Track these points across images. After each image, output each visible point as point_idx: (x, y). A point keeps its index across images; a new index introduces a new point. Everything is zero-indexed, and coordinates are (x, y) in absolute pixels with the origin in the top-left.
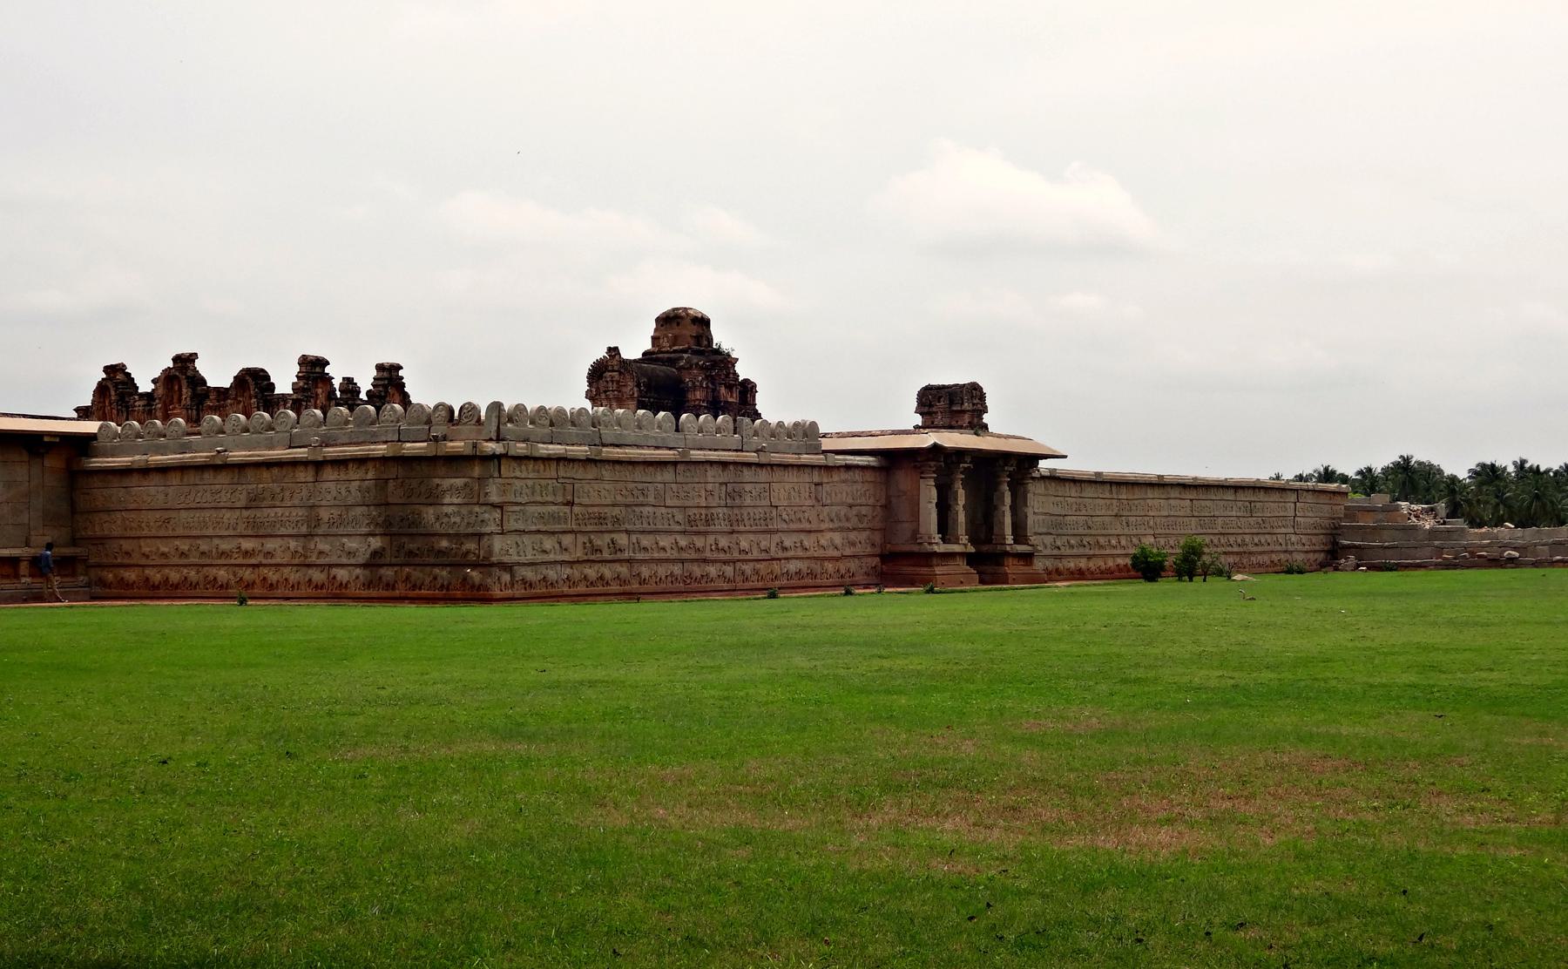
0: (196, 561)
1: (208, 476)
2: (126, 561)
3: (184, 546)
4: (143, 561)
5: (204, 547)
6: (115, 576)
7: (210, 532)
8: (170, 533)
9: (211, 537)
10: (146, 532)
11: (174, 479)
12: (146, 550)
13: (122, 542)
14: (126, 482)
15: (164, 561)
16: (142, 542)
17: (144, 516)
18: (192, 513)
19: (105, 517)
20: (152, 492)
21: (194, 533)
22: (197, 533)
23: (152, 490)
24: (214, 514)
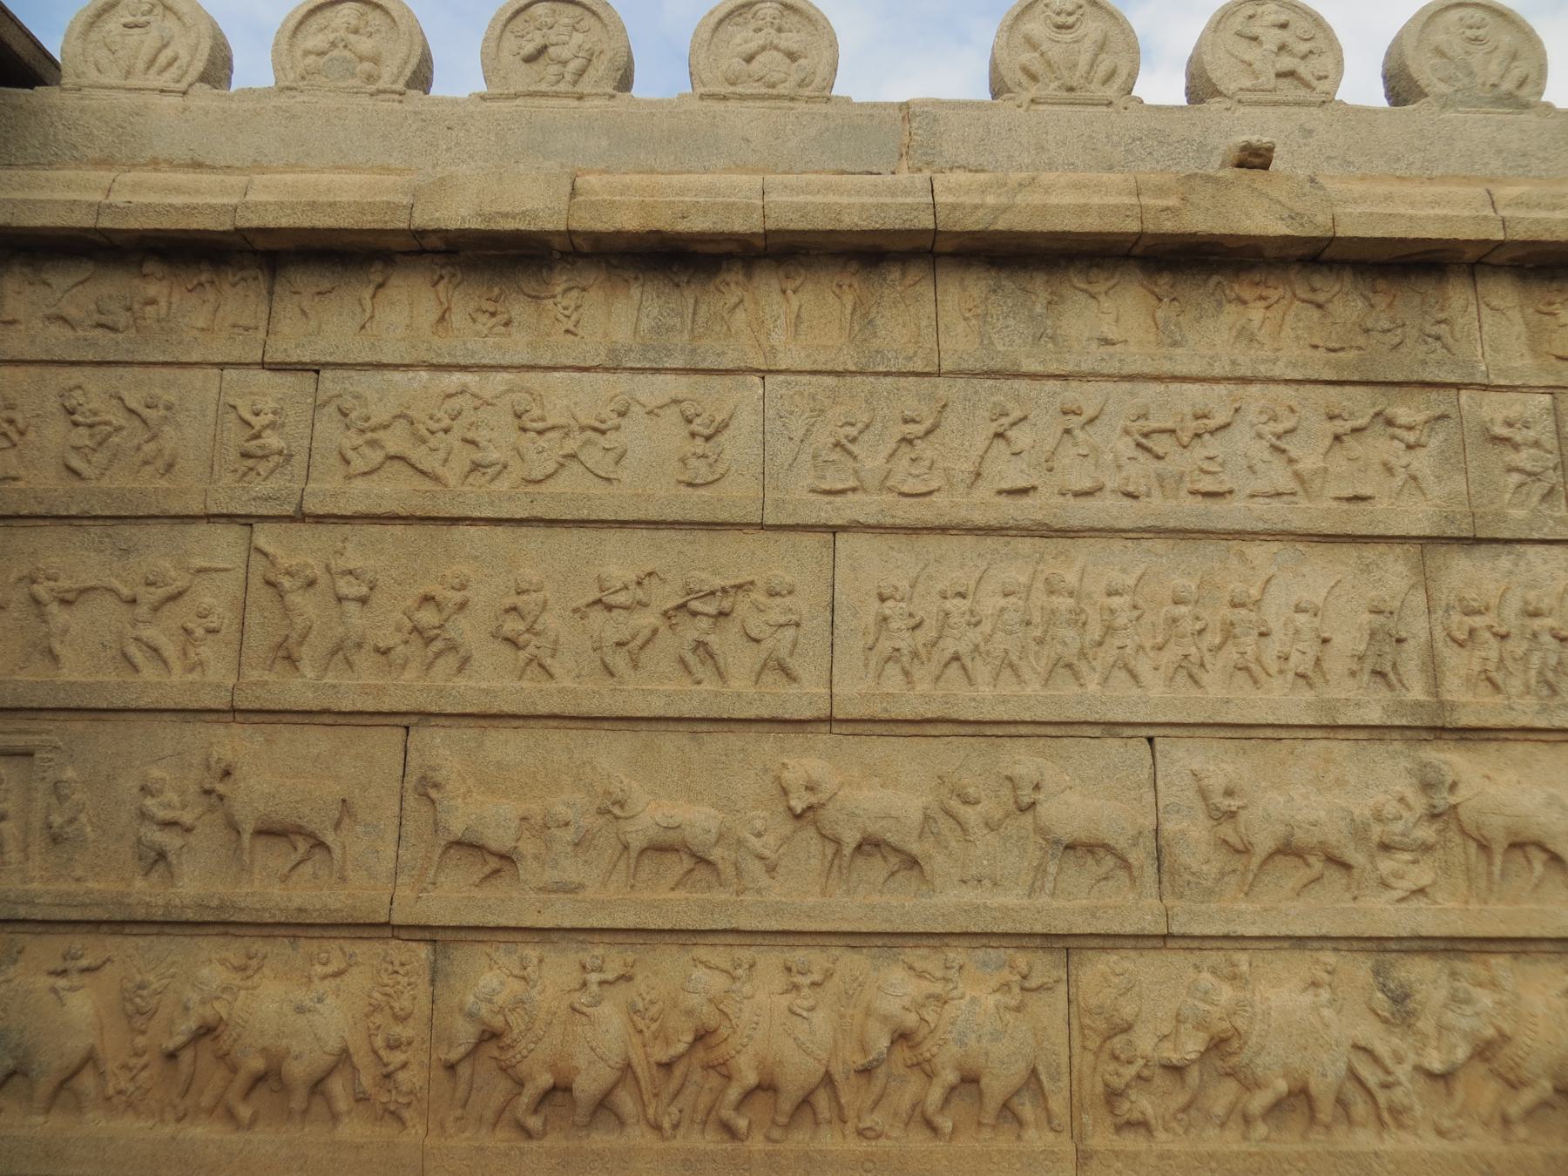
0: (1010, 904)
1: (1111, 320)
2: (270, 886)
3: (885, 790)
4: (451, 896)
5: (1084, 793)
6: (134, 1011)
7: (1155, 696)
8: (742, 690)
9: (1151, 734)
10: (492, 680)
11: (791, 322)
12: (478, 810)
13: (231, 742)
14: (323, 320)
15: (668, 899)
16: (440, 749)
17: (480, 567)
18: (956, 562)
19: (73, 560)
20: (581, 388)
21: (984, 696)
22: (1031, 695)
23: (566, 398)
24: (1178, 570)
